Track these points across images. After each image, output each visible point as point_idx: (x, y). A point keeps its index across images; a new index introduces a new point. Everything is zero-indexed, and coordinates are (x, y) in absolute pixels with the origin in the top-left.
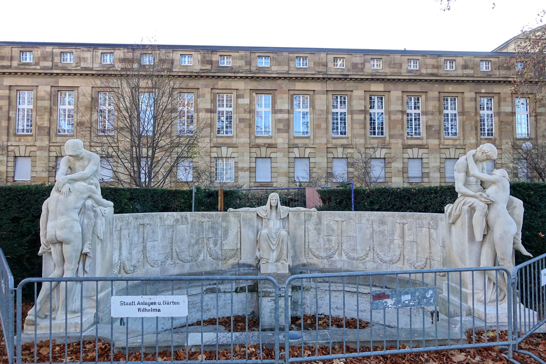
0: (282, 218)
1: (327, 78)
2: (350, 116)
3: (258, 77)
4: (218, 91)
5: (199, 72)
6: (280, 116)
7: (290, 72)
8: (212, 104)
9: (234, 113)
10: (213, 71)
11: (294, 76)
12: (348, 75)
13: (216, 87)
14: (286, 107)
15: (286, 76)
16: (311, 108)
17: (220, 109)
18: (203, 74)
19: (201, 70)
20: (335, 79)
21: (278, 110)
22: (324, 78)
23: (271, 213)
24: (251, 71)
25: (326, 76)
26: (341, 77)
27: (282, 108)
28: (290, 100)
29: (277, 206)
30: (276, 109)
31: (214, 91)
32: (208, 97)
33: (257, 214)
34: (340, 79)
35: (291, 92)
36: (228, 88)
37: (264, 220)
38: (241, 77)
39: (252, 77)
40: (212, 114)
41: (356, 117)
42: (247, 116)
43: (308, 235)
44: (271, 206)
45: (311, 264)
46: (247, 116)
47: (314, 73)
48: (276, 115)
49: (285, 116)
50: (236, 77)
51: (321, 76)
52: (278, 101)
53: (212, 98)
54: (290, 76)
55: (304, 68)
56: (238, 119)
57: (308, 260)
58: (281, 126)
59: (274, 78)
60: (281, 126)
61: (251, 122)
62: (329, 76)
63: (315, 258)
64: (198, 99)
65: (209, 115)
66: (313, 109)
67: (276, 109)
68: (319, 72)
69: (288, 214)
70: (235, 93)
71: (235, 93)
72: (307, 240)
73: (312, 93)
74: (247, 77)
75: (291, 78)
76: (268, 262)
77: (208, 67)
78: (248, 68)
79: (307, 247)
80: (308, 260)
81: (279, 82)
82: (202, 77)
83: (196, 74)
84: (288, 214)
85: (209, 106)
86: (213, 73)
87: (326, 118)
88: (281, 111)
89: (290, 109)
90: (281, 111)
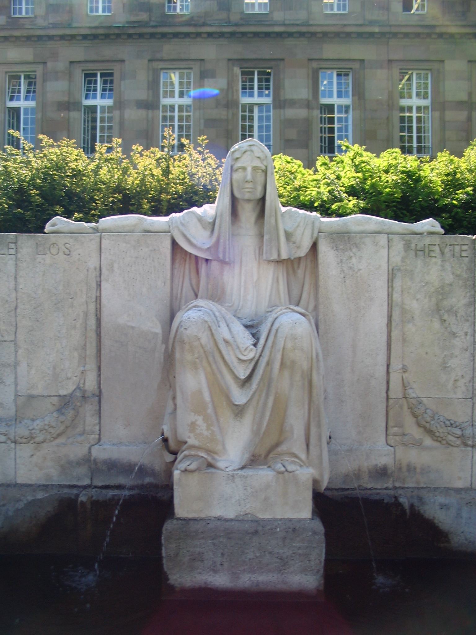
0: (284, 256)
1: (390, 33)
2: (437, 114)
3: (244, 34)
4: (161, 65)
5: (123, 27)
6: (290, 113)
7: (311, 22)
8: (151, 92)
9: (195, 109)
10: (152, 24)
11: (319, 30)
12: (434, 27)
13: (159, 56)
14: (304, 93)
15: (304, 29)
16: (356, 98)
17: (166, 101)
18: (131, 31)
19: (128, 22)
20: (406, 35)
21: (285, 101)
22: (383, 34)
23: (234, 235)
24: (230, 22)
25: (387, 29)
26: (419, 30)
27: (295, 97)
28: (310, 81)
29: (263, 200)
30: (282, 98)
31: (157, 65)
32: (143, 76)
33: (174, 243)
34: (418, 35)
35: (315, 65)
36: (183, 56)
37: (203, 268)
38: (210, 35)
39: (232, 34)
40: (150, 112)
41: (450, 115)
42: (222, 113)
43: (404, 340)
44: (234, 200)
45: (411, 469)
46: (222, 113)
47: (360, 22)
48: (282, 111)
49: (302, 113)
50: (198, 35)
51: (376, 30)
52: (287, 83)
53: (151, 79)
54: (312, 29)
55: (341, 14)
56: (202, 121)
57: (400, 452)
58: (292, 134)
59: (279, 35)
60: (292, 134)
61: (230, 127)
62: (394, 30)
63: (428, 441)
64: (123, 82)
65: (141, 113)
66: (359, 98)
67: (282, 98)
68: (372, 23)
69: (314, 247)
70: (197, 67)
71: (197, 67)
72: (396, 365)
73: (356, 66)
74: (222, 35)
75: (313, 34)
76: (210, 465)
77: (144, 16)
78: (223, 15)
79: (396, 390)
80: (400, 452)
81: (289, 42)
82: (130, 36)
83: (117, 31)
84: (314, 247)
85: (143, 95)
86: (153, 27)
87: (388, 118)
88: (292, 103)
89: (311, 98)
90: (292, 103)
